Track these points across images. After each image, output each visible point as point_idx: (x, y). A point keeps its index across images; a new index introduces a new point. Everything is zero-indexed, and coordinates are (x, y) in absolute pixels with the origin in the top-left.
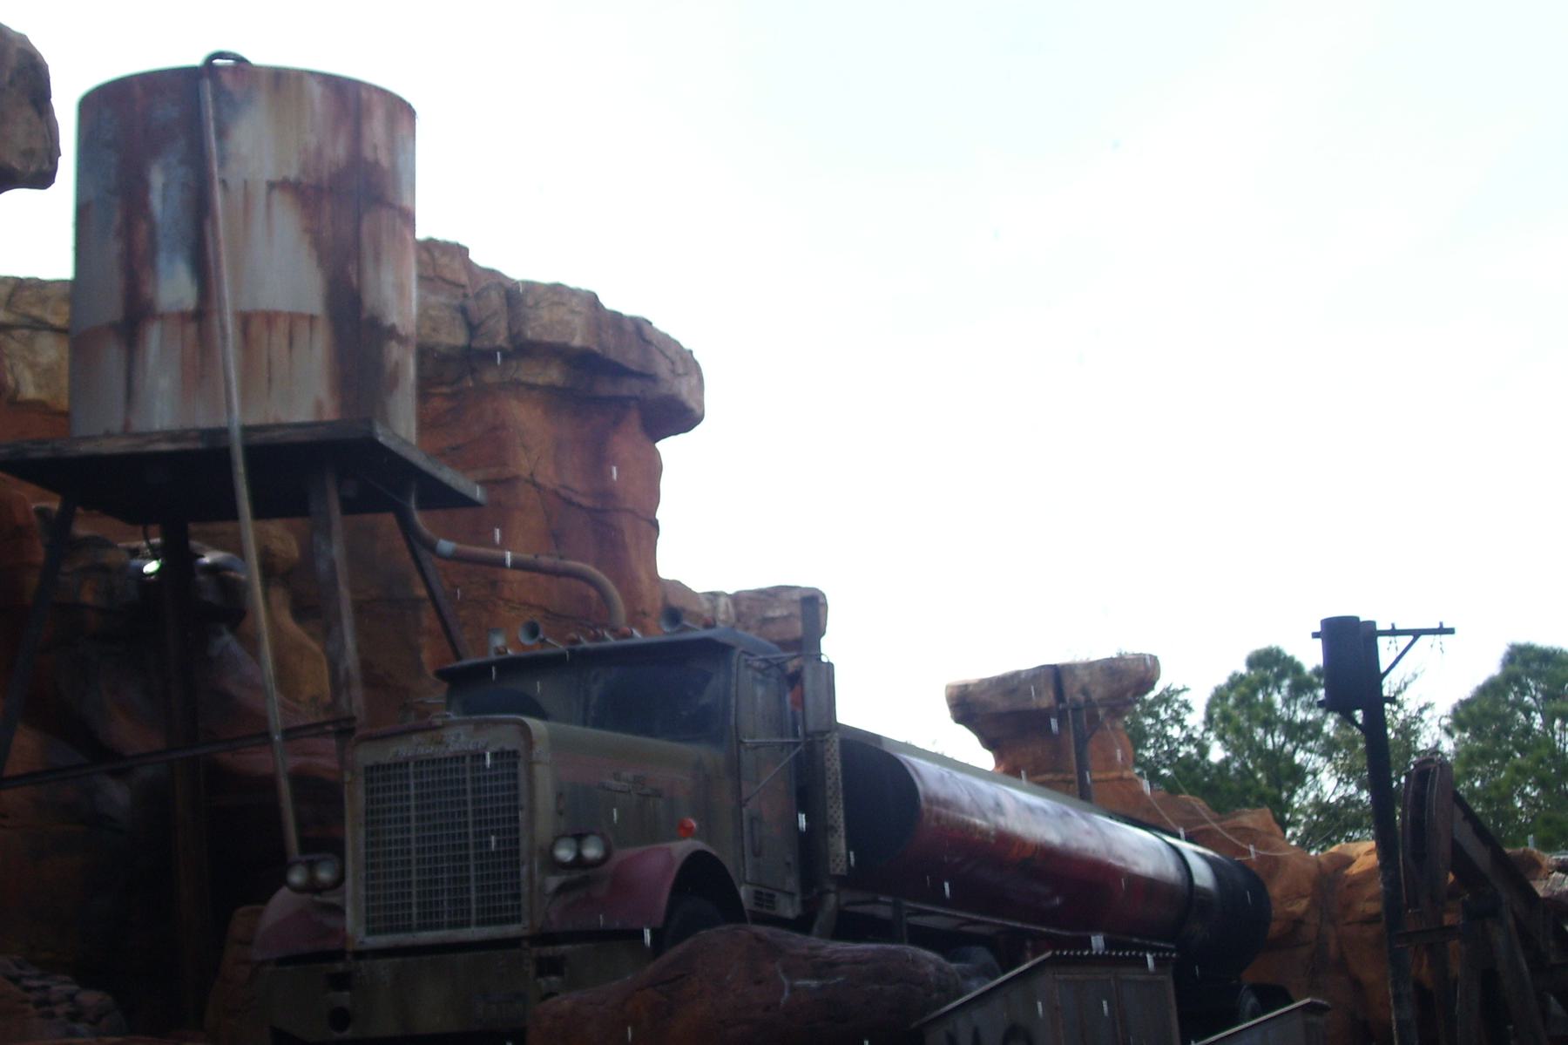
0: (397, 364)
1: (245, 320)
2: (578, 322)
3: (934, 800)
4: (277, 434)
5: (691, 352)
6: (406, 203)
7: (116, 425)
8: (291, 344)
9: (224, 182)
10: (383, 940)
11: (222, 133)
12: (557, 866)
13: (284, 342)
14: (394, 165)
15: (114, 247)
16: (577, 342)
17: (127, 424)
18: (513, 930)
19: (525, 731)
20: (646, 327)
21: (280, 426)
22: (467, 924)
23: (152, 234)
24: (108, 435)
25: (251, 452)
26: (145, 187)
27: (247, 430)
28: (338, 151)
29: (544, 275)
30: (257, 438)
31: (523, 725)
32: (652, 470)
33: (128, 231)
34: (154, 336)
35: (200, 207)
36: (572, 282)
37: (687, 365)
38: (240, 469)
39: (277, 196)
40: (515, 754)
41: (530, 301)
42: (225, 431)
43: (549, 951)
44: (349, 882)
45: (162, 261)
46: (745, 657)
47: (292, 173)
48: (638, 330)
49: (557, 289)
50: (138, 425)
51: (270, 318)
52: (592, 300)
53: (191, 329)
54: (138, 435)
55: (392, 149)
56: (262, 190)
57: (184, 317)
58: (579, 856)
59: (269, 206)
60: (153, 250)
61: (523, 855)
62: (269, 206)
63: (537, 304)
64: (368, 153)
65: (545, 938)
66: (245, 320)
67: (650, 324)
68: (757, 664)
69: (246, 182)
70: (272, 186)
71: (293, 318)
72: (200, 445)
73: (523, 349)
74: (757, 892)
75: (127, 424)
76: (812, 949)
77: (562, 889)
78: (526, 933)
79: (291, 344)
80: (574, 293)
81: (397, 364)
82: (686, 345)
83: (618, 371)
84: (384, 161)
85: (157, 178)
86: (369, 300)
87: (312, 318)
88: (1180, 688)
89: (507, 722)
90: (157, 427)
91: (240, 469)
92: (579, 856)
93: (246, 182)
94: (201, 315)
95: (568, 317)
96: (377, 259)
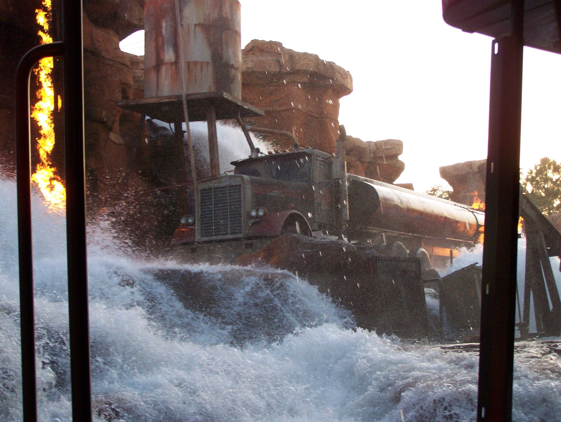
0: (234, 75)
1: (188, 64)
2: (312, 64)
3: (385, 199)
4: (193, 97)
5: (349, 71)
6: (237, 29)
7: (154, 95)
8: (202, 70)
9: (182, 25)
10: (206, 239)
11: (181, 11)
12: (251, 217)
13: (200, 70)
14: (232, 18)
15: (153, 45)
16: (311, 69)
17: (157, 95)
18: (240, 236)
19: (243, 178)
20: (333, 65)
21: (199, 94)
22: (227, 234)
23: (163, 41)
24: (152, 97)
25: (188, 101)
26: (161, 27)
27: (187, 95)
28: (215, 15)
29: (302, 50)
30: (190, 98)
31: (242, 177)
32: (336, 106)
33: (156, 40)
34: (163, 69)
35: (175, 33)
36: (310, 52)
37: (346, 75)
38: (185, 106)
39: (197, 28)
40: (240, 185)
41: (297, 58)
42: (181, 96)
43: (249, 242)
44: (196, 222)
45: (166, 47)
46: (315, 157)
47: (202, 21)
48: (331, 66)
49: (305, 54)
50: (160, 94)
51: (196, 63)
52: (316, 57)
53: (174, 67)
54: (159, 97)
55: (232, 15)
56: (193, 27)
57: (172, 64)
58: (257, 214)
59: (195, 32)
60: (163, 45)
61: (242, 214)
62: (195, 32)
63: (300, 58)
64: (224, 15)
65: (249, 238)
66: (188, 64)
67: (335, 63)
68: (320, 159)
69: (188, 24)
70: (196, 25)
71: (202, 63)
72: (176, 100)
73: (295, 72)
74: (319, 225)
75: (157, 95)
76: (311, 240)
77: (253, 224)
78: (243, 236)
79: (202, 70)
80: (311, 55)
81: (234, 75)
82: (346, 69)
83: (325, 78)
84: (230, 18)
85: (164, 24)
86: (225, 56)
87: (208, 63)
88: (43, 151)
89: (238, 177)
90: (165, 95)
91: (185, 106)
92: (257, 214)
93: (188, 24)
94: (176, 63)
95: (309, 62)
96: (227, 45)
